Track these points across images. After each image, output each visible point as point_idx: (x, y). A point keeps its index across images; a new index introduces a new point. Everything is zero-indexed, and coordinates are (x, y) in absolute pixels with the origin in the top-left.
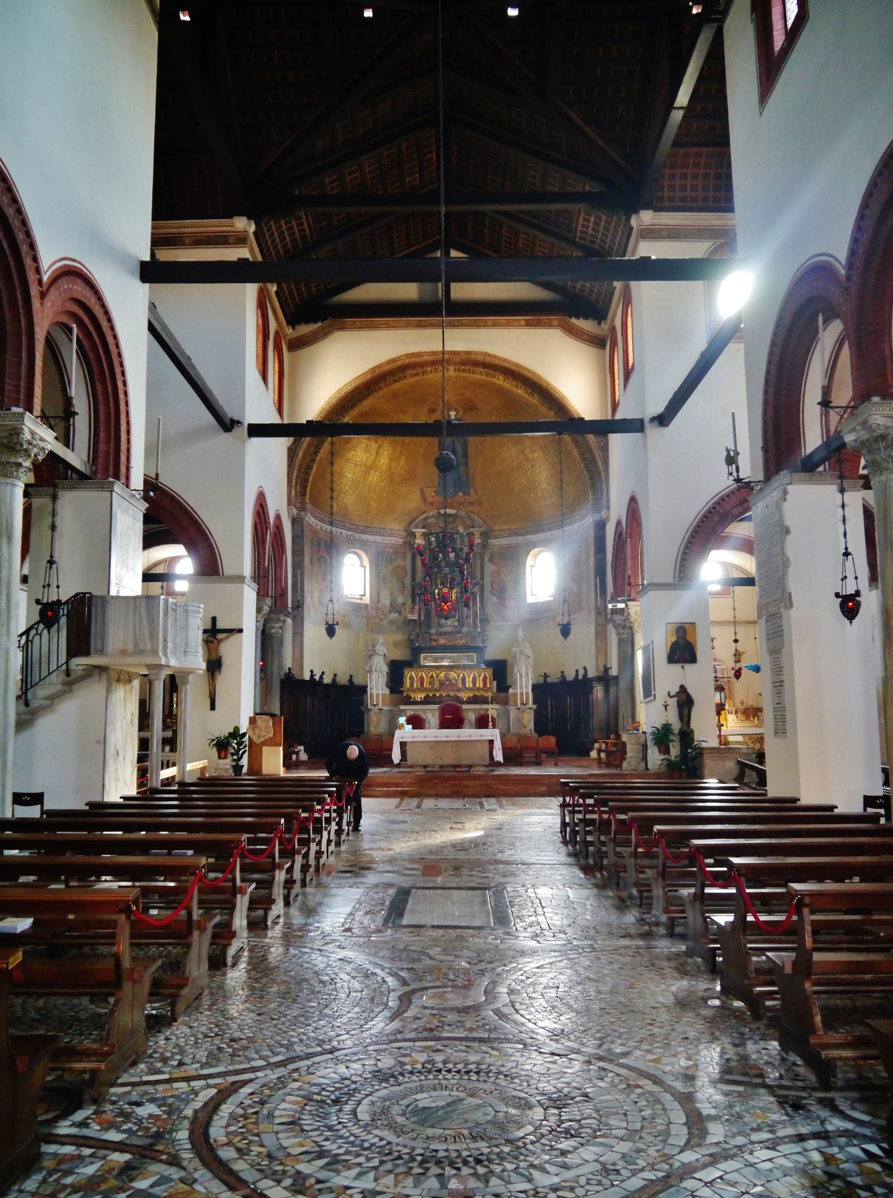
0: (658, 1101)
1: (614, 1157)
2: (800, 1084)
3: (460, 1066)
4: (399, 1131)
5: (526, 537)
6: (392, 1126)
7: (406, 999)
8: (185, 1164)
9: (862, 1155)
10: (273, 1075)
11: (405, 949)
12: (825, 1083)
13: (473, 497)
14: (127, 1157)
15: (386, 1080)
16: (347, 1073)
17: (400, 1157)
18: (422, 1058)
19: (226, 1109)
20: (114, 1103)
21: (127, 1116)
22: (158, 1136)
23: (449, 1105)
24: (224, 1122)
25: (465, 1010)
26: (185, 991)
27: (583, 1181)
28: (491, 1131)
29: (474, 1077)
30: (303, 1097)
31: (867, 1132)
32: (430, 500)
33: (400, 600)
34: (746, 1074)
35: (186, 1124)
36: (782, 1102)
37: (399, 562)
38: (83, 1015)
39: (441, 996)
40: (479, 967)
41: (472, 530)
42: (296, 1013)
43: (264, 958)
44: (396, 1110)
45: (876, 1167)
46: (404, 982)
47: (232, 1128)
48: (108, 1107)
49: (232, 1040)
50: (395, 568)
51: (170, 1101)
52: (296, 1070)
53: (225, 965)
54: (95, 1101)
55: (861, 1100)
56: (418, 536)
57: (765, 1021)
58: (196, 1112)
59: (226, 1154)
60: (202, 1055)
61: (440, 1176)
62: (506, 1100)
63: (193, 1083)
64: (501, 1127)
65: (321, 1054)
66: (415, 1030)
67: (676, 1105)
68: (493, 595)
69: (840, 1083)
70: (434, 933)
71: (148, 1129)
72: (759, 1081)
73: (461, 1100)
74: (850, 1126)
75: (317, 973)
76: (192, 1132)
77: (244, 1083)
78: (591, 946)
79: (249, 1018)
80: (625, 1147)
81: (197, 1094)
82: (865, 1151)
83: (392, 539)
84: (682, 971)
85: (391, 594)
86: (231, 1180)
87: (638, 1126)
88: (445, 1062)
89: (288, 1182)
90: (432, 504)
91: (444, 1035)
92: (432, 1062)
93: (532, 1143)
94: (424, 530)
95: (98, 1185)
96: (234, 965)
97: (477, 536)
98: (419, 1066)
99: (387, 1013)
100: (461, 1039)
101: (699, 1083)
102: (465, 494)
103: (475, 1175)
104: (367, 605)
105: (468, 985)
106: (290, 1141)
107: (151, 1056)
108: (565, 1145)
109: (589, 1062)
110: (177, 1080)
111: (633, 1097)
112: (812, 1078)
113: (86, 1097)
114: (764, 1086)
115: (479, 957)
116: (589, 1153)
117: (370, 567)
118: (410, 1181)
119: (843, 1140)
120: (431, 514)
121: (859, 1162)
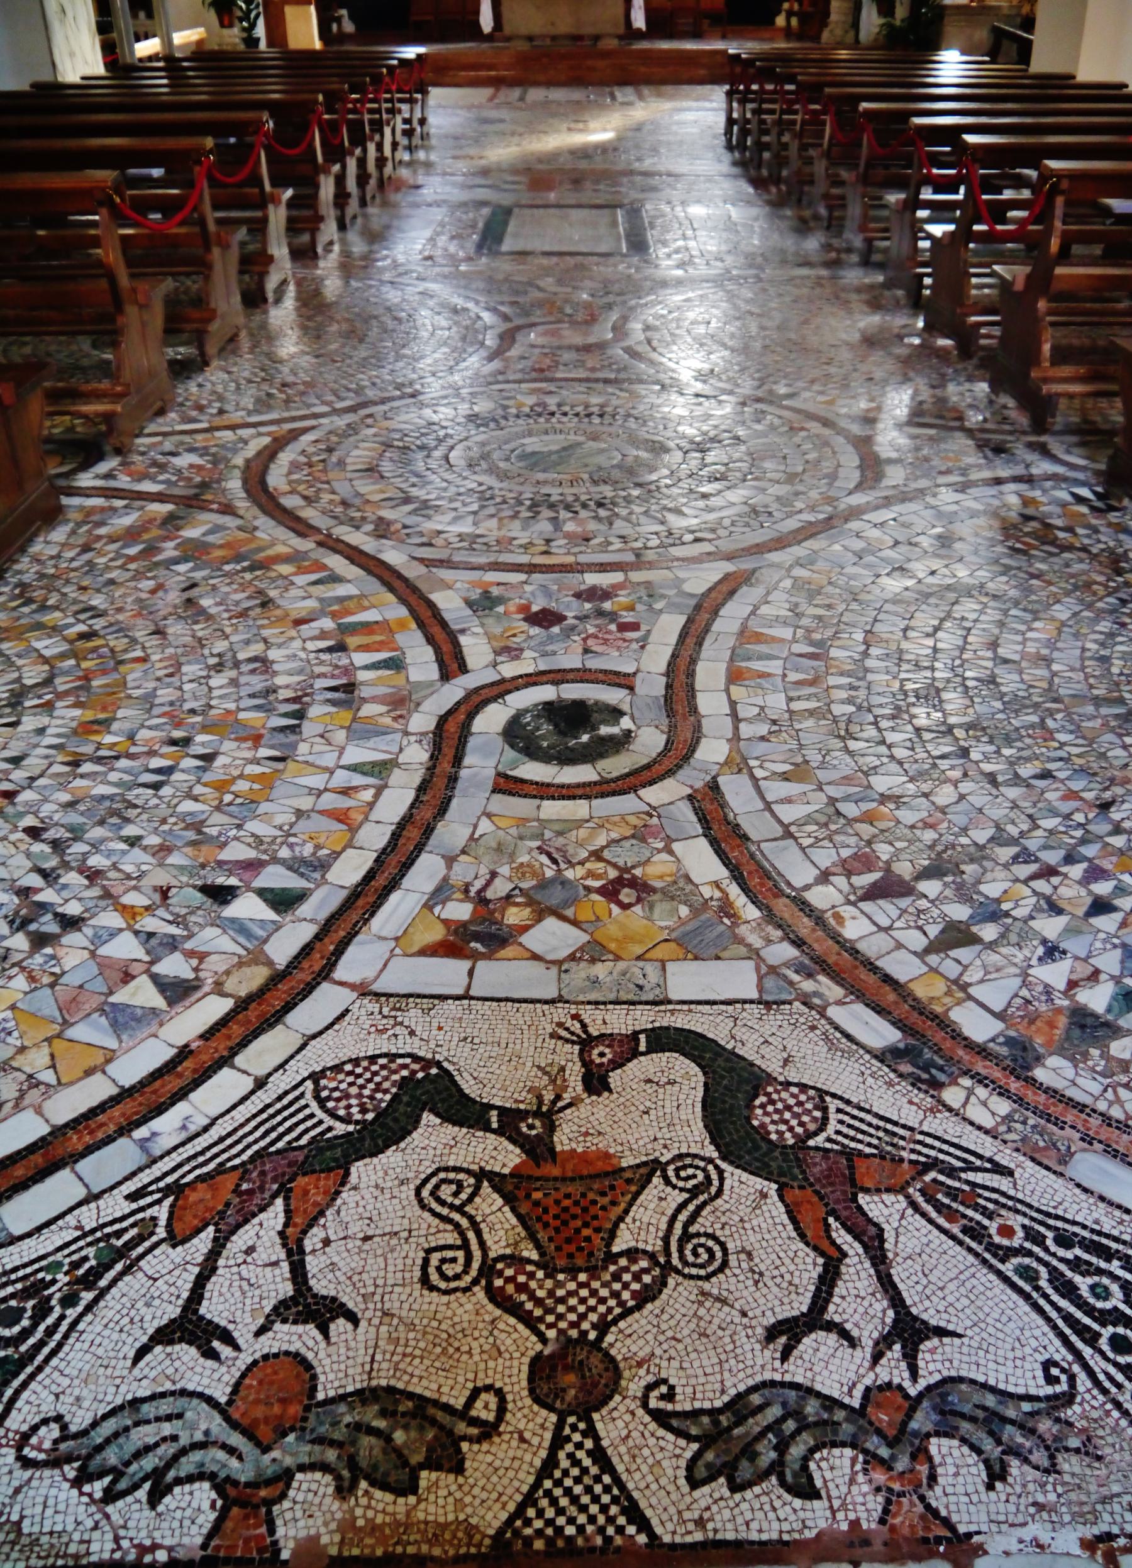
0: (826, 444)
1: (768, 500)
2: (1007, 427)
3: (579, 409)
4: (503, 476)
6: (493, 470)
7: (508, 338)
8: (241, 512)
9: (1069, 498)
10: (341, 422)
11: (506, 280)
12: (1040, 425)
14: (169, 507)
15: (486, 425)
16: (435, 418)
17: (504, 502)
18: (531, 400)
19: (285, 457)
20: (143, 454)
21: (162, 467)
22: (204, 486)
23: (564, 449)
24: (285, 470)
25: (587, 349)
26: (214, 327)
27: (727, 522)
28: (616, 474)
29: (596, 420)
30: (383, 444)
31: (1080, 476)
34: (941, 417)
35: (237, 473)
36: (981, 446)
38: (85, 362)
39: (554, 333)
40: (605, 300)
42: (364, 354)
43: (317, 293)
44: (496, 455)
45: (1084, 510)
46: (506, 318)
47: (295, 477)
48: (137, 458)
49: (284, 385)
51: (213, 450)
52: (370, 416)
53: (265, 300)
54: (118, 451)
55: (1082, 444)
57: (975, 361)
58: (248, 461)
59: (290, 502)
60: (248, 402)
61: (554, 520)
62: (634, 441)
63: (240, 432)
64: (631, 472)
65: (401, 398)
66: (522, 371)
67: (850, 448)
69: (1057, 427)
70: (545, 261)
71: (190, 479)
72: (957, 424)
73: (579, 444)
74: (1060, 470)
75: (389, 309)
76: (245, 481)
77: (305, 431)
78: (757, 276)
79: (306, 361)
80: (783, 490)
81: (246, 442)
82: (1074, 495)
84: (875, 305)
86: (300, 527)
87: (800, 469)
88: (559, 405)
89: (370, 527)
91: (559, 375)
92: (544, 405)
93: (667, 486)
95: (139, 534)
96: (278, 301)
98: (527, 410)
99: (483, 353)
100: (580, 380)
101: (880, 426)
103: (597, 518)
105: (592, 320)
106: (367, 487)
107: (182, 405)
108: (706, 489)
109: (744, 404)
110: (218, 429)
111: (797, 440)
112: (1023, 421)
113: (108, 448)
114: (963, 429)
115: (606, 286)
116: (736, 496)
118: (517, 524)
119: (1049, 484)
121: (1064, 505)
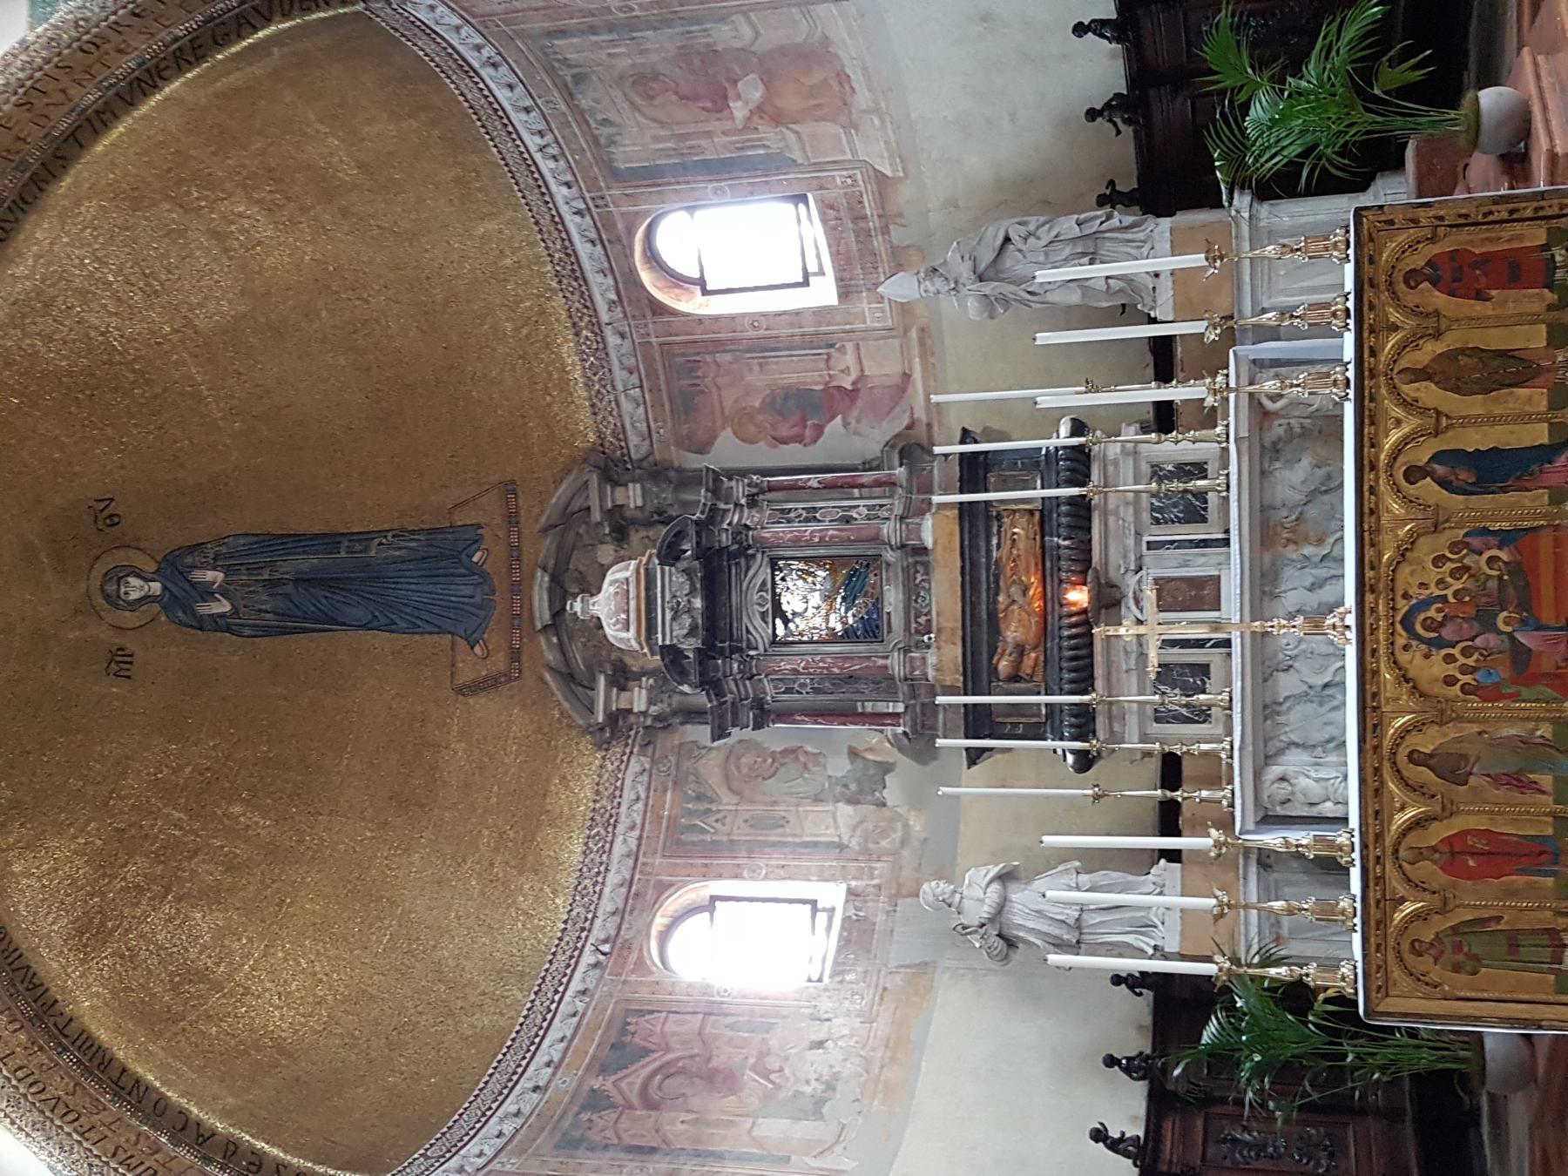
5: (605, 318)
13: (488, 513)
32: (500, 661)
33: (840, 766)
37: (710, 768)
41: (596, 516)
50: (727, 777)
56: (621, 701)
68: (819, 430)
83: (628, 795)
85: (818, 799)
90: (515, 655)
94: (602, 682)
97: (620, 496)
102: (478, 540)
104: (851, 893)
117: (720, 876)
120: (551, 657)
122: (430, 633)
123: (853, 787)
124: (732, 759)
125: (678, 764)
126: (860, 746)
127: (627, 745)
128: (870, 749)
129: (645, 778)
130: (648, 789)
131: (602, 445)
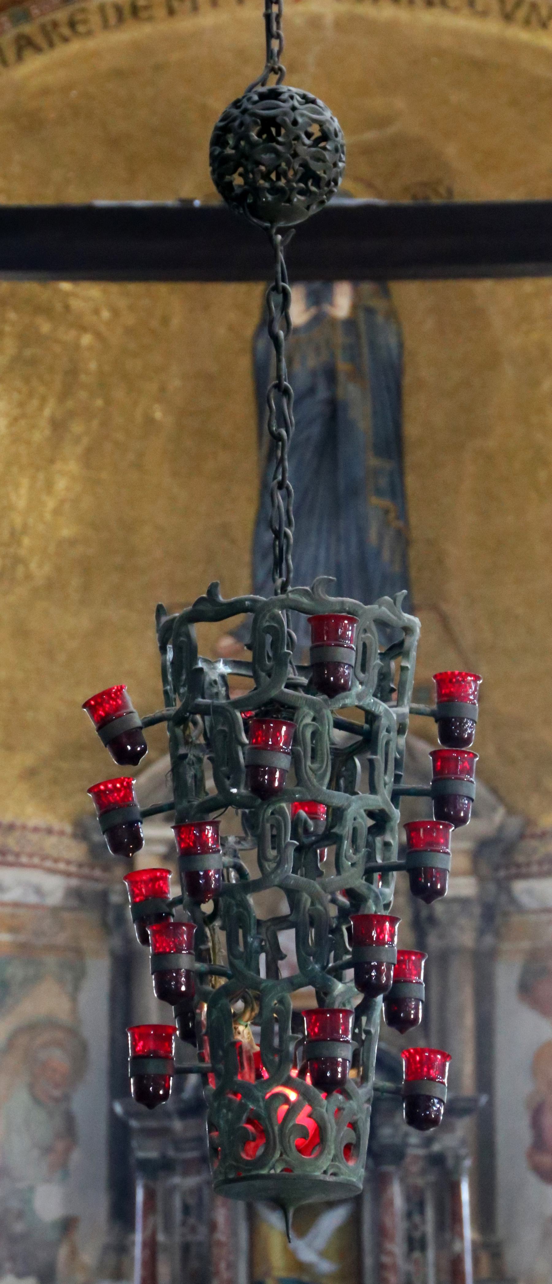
122: (254, 576)
123: (19, 1227)
124: (59, 1035)
125: (51, 948)
126: (81, 1233)
127: (80, 865)
128: (74, 1253)
129: (32, 899)
130: (16, 905)
131: (533, 836)
